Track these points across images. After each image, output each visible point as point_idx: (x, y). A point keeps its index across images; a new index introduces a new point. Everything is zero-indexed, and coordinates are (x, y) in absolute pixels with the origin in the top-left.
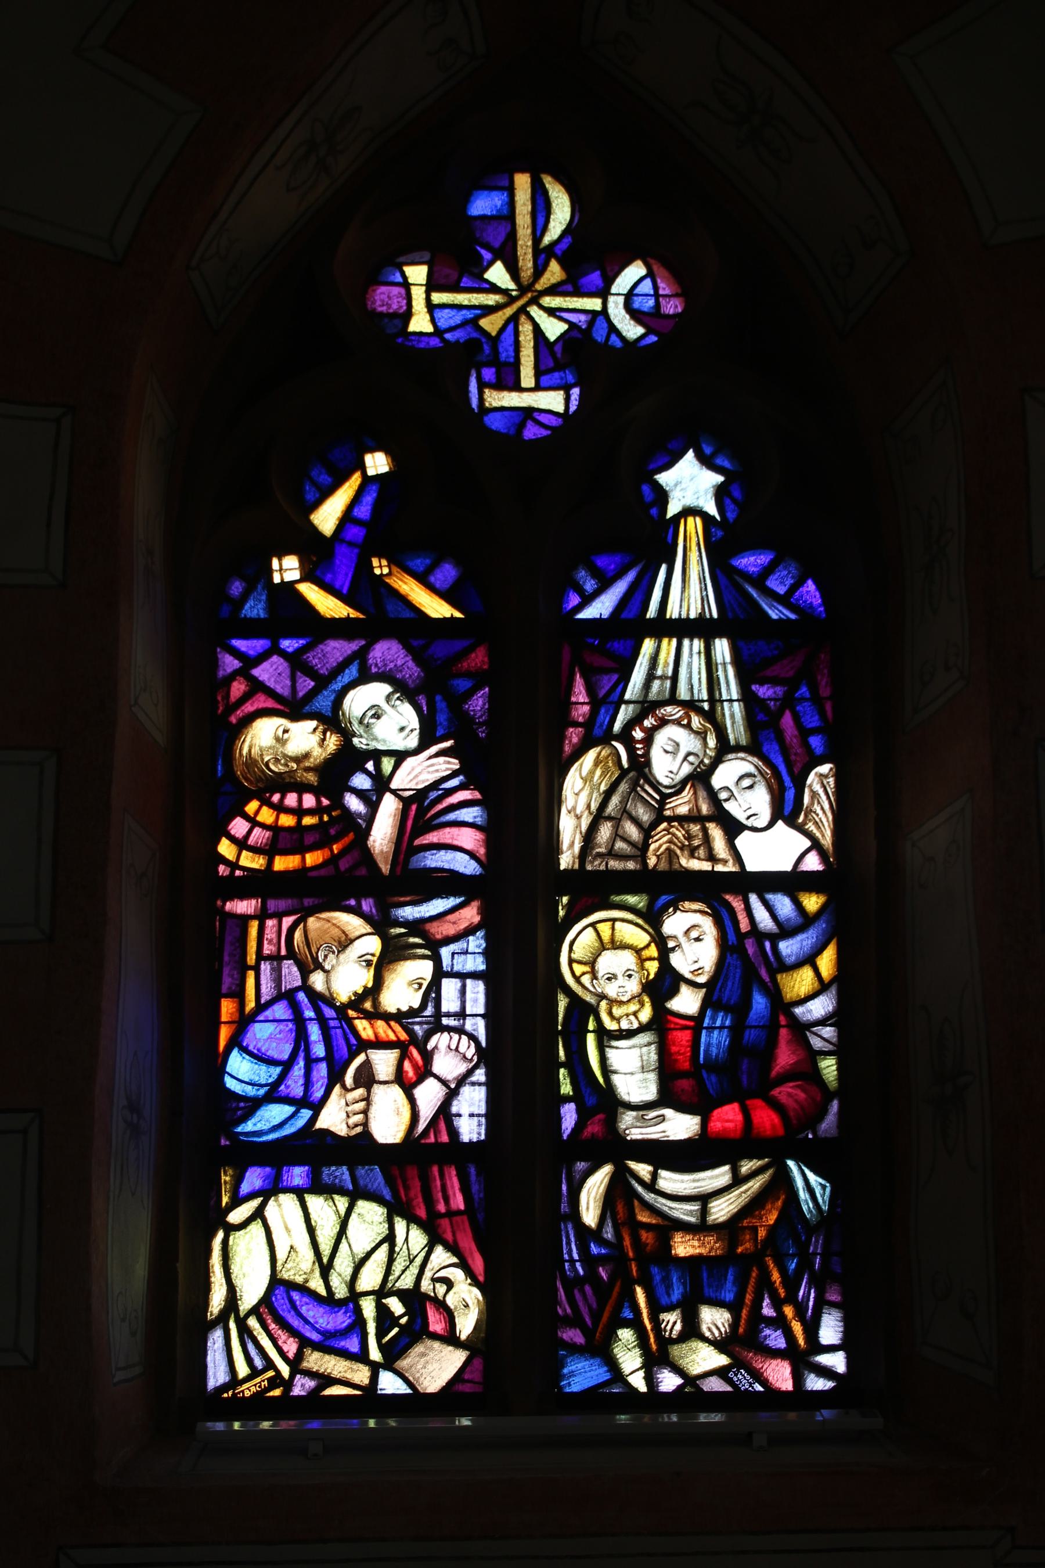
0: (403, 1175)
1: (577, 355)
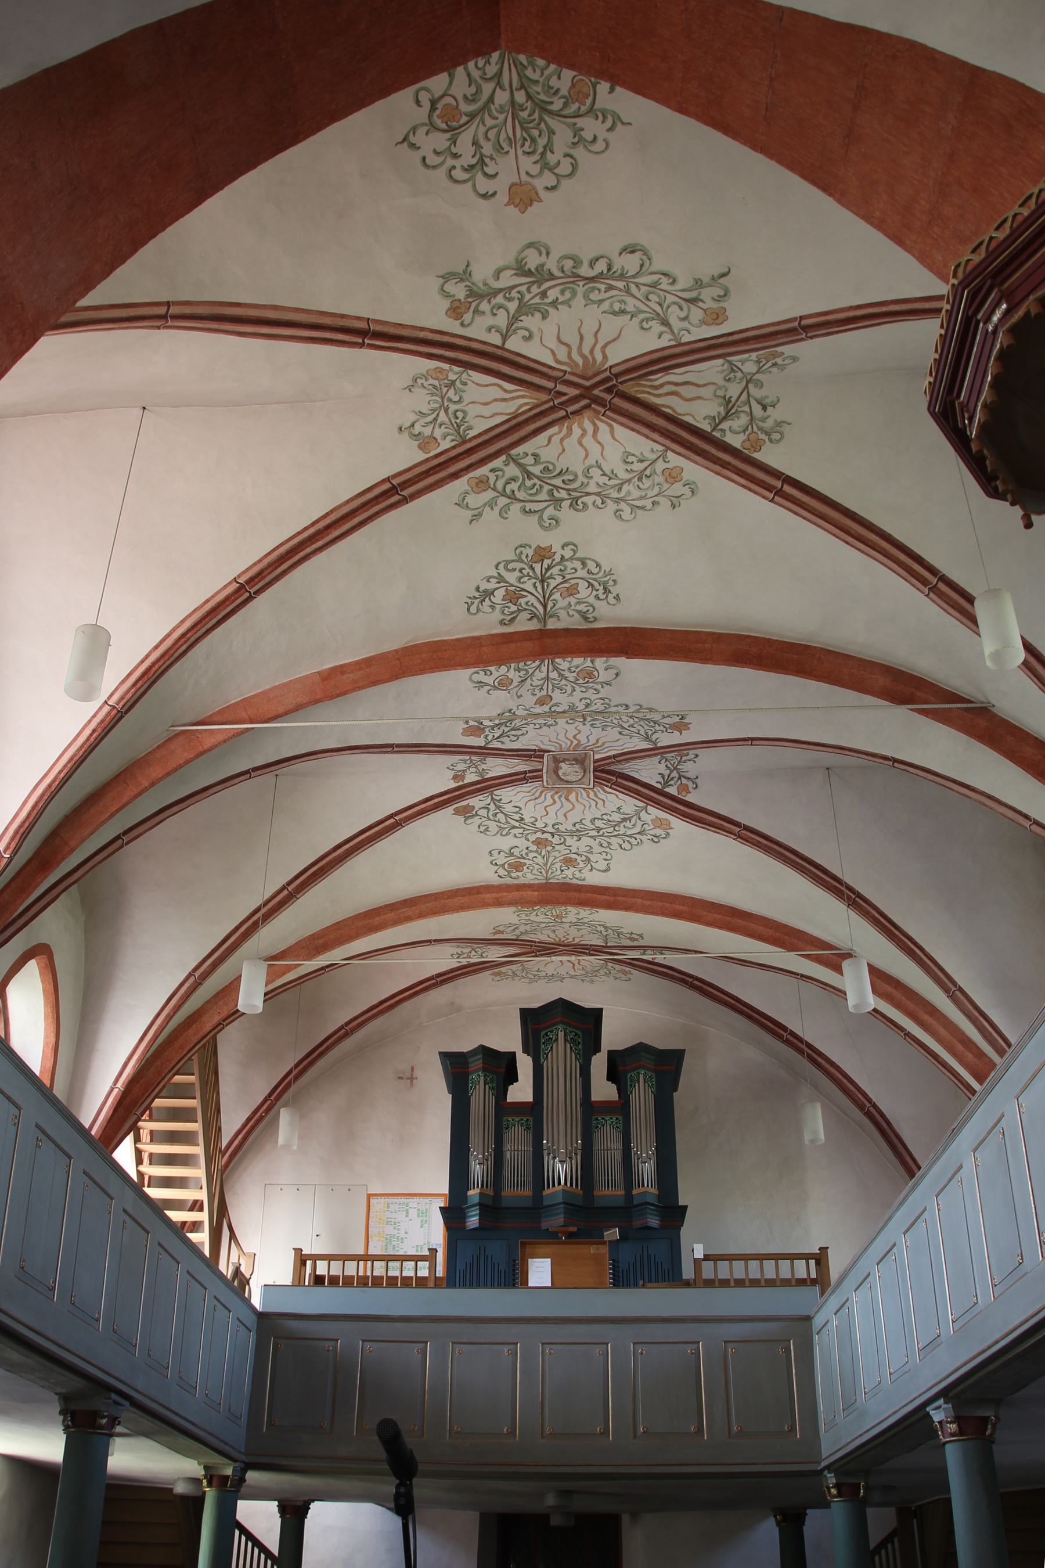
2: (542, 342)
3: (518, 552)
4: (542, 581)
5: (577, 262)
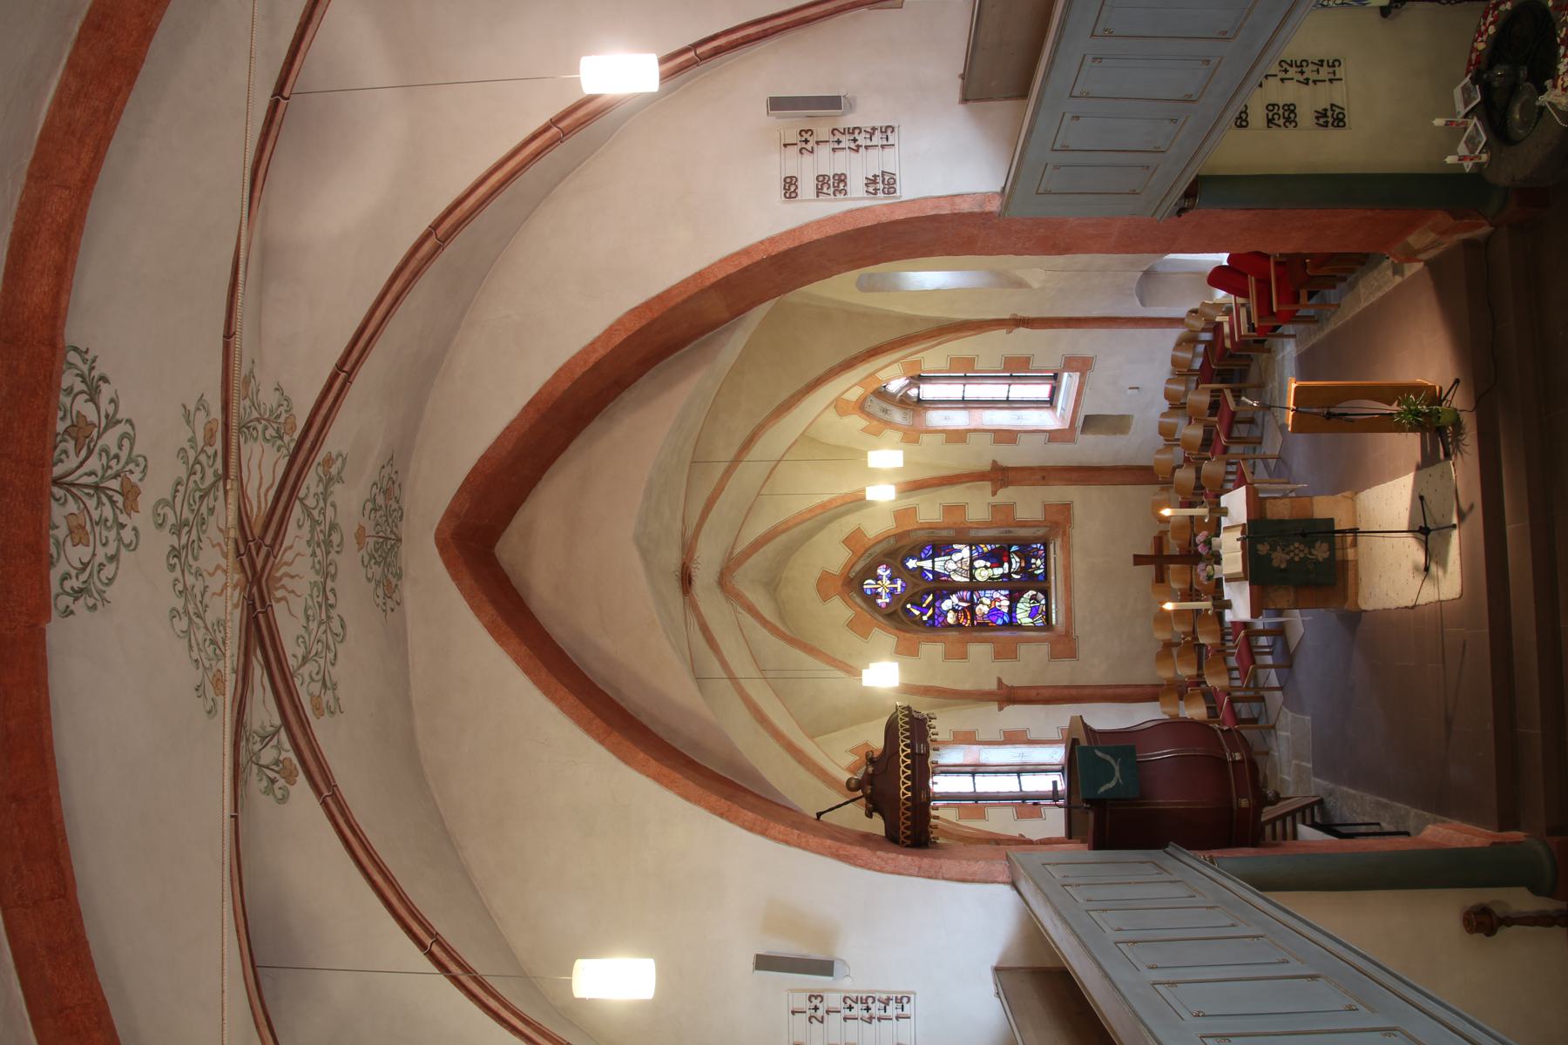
0: (1014, 600)
1: (892, 579)
2: (296, 536)
3: (141, 460)
4: (96, 487)
5: (334, 577)
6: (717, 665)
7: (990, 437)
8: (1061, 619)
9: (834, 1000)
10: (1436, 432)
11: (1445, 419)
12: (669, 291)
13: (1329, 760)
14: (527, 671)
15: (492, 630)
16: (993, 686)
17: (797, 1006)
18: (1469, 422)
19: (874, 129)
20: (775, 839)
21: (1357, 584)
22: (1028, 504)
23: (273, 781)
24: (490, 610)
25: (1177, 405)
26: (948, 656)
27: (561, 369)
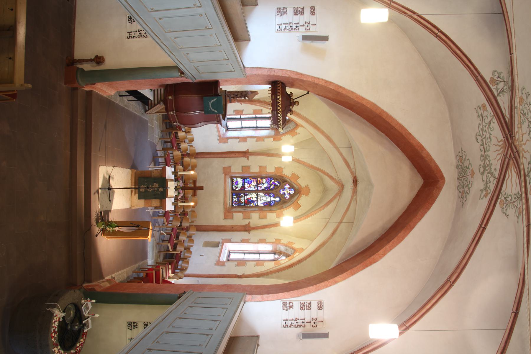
0: (243, 187)
1: (285, 194)
6: (344, 154)
7: (251, 241)
8: (228, 180)
9: (302, 29)
10: (104, 217)
11: (101, 224)
12: (364, 268)
13: (143, 125)
14: (410, 134)
15: (423, 148)
16: (250, 157)
17: (314, 27)
18: (94, 222)
19: (290, 327)
20: (323, 80)
21: (132, 178)
22: (238, 219)
23: (498, 77)
24: (424, 155)
25: (187, 249)
26: (265, 167)
27: (402, 241)
